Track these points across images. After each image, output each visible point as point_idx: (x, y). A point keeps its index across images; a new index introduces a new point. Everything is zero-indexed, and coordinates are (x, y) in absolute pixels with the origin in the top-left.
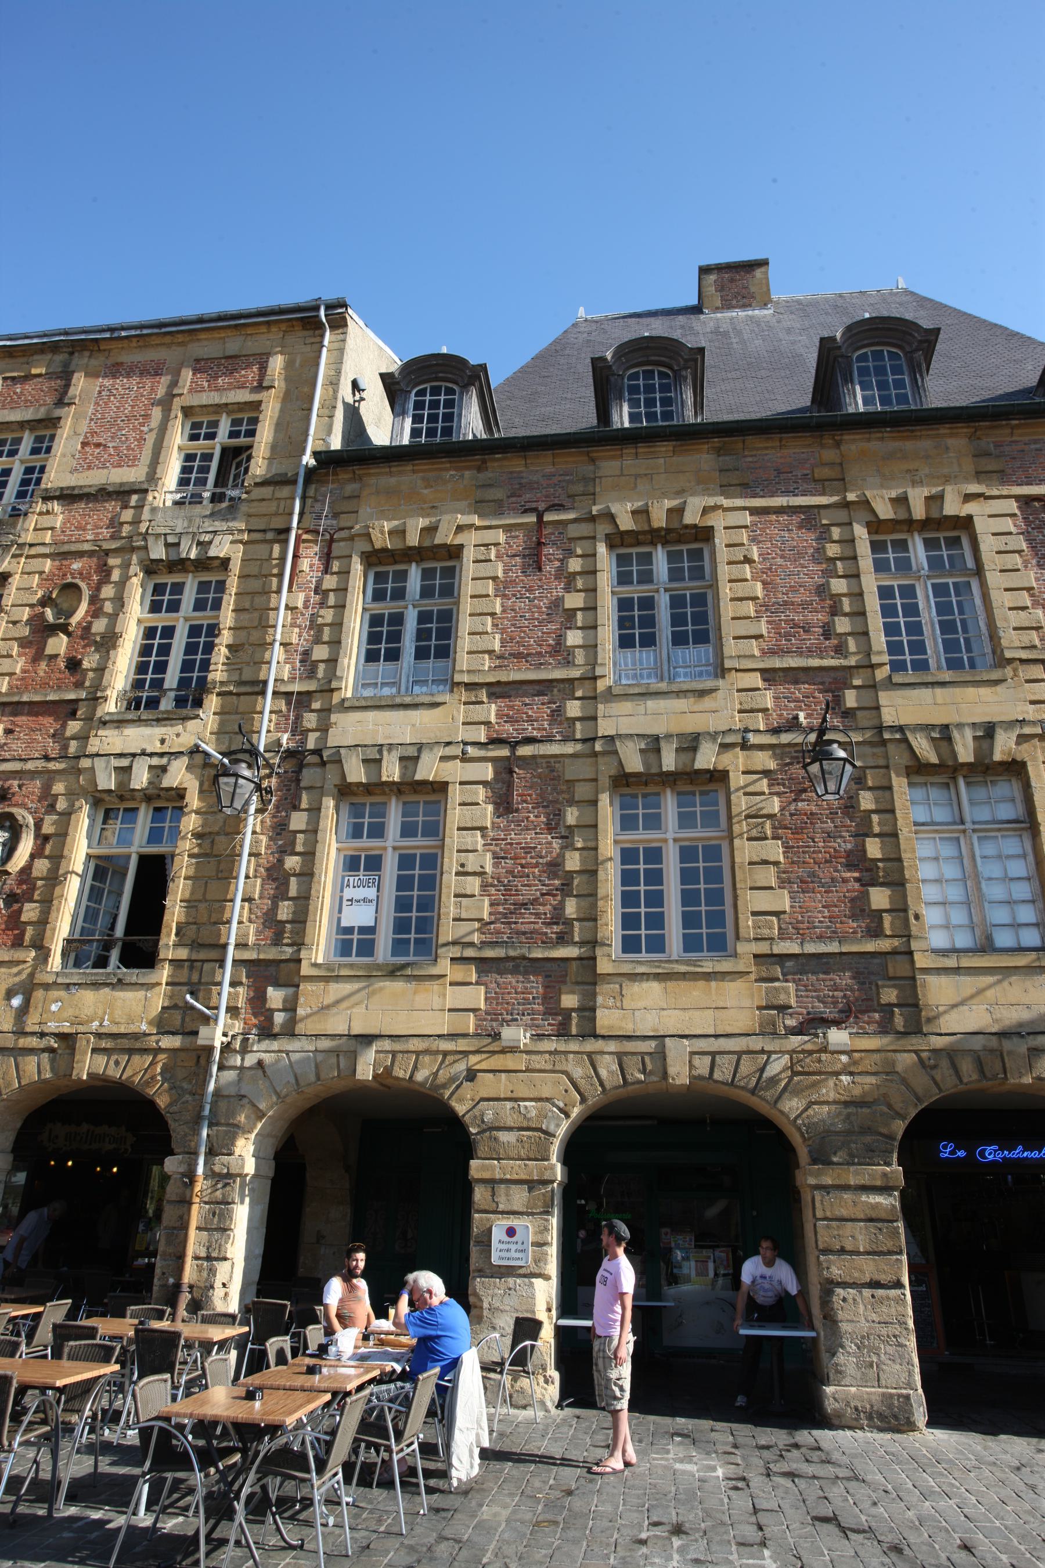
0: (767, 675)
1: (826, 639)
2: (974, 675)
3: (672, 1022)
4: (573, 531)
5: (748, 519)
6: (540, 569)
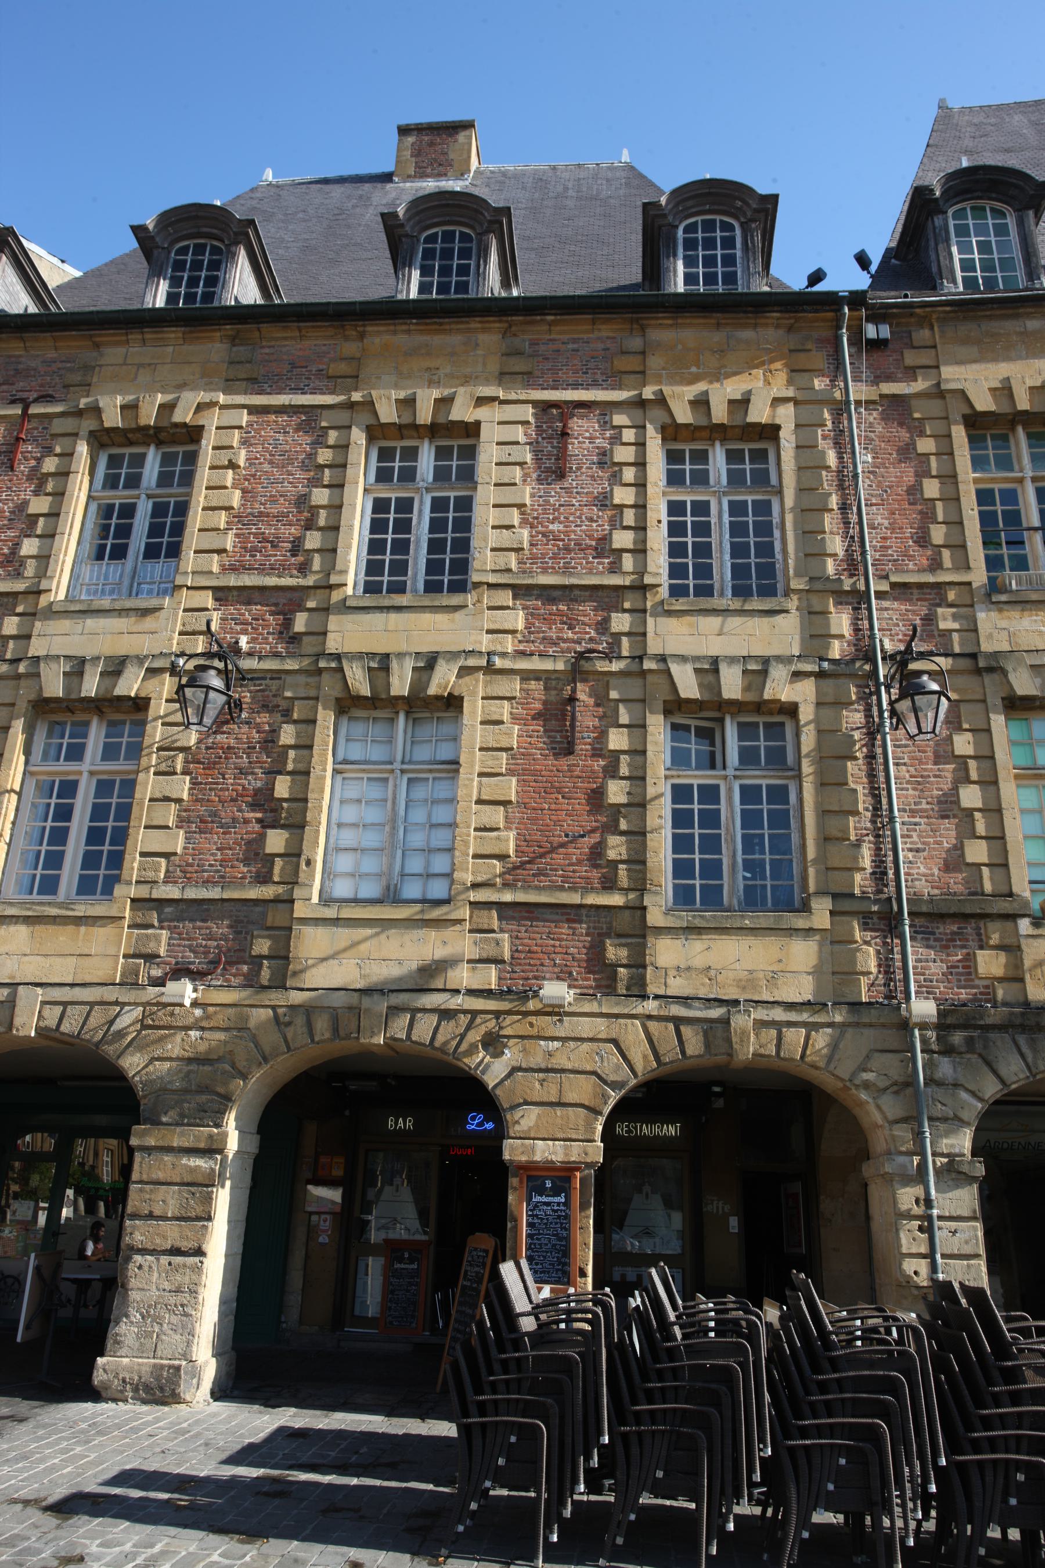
0: (220, 594)
1: (293, 555)
2: (433, 600)
3: (32, 969)
4: (59, 426)
5: (244, 418)
6: (12, 468)
